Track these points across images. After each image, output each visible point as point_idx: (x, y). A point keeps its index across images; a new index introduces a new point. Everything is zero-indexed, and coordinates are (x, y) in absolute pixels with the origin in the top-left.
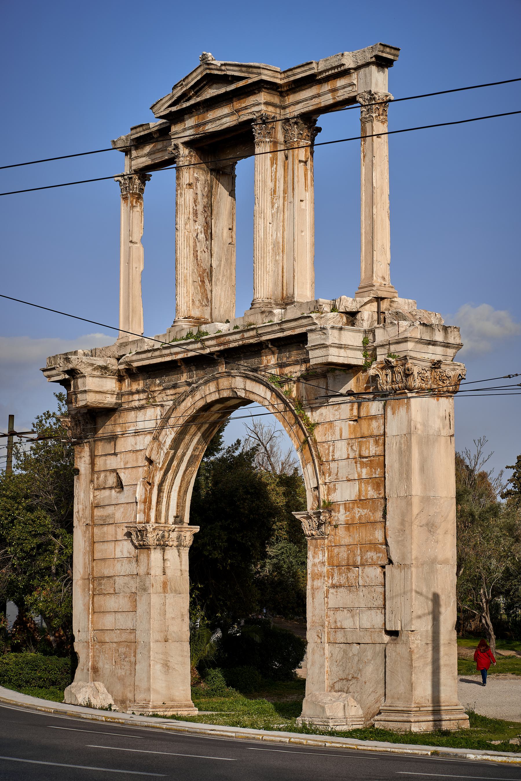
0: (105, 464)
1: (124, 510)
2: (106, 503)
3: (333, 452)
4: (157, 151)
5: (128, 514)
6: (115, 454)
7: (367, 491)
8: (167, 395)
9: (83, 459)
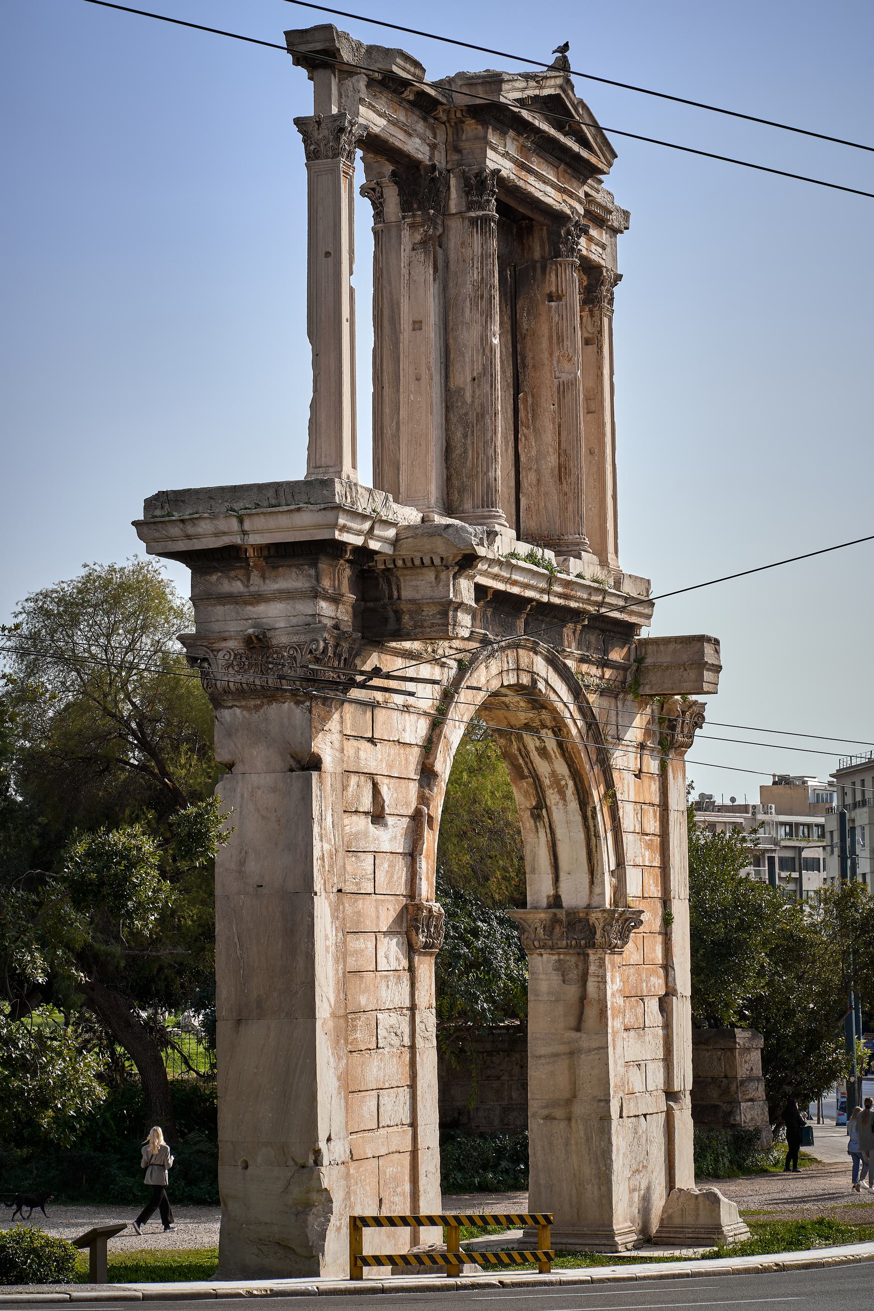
1: (389, 867)
2: (362, 845)
4: (400, 124)
5: (395, 878)
6: (372, 740)
8: (451, 647)
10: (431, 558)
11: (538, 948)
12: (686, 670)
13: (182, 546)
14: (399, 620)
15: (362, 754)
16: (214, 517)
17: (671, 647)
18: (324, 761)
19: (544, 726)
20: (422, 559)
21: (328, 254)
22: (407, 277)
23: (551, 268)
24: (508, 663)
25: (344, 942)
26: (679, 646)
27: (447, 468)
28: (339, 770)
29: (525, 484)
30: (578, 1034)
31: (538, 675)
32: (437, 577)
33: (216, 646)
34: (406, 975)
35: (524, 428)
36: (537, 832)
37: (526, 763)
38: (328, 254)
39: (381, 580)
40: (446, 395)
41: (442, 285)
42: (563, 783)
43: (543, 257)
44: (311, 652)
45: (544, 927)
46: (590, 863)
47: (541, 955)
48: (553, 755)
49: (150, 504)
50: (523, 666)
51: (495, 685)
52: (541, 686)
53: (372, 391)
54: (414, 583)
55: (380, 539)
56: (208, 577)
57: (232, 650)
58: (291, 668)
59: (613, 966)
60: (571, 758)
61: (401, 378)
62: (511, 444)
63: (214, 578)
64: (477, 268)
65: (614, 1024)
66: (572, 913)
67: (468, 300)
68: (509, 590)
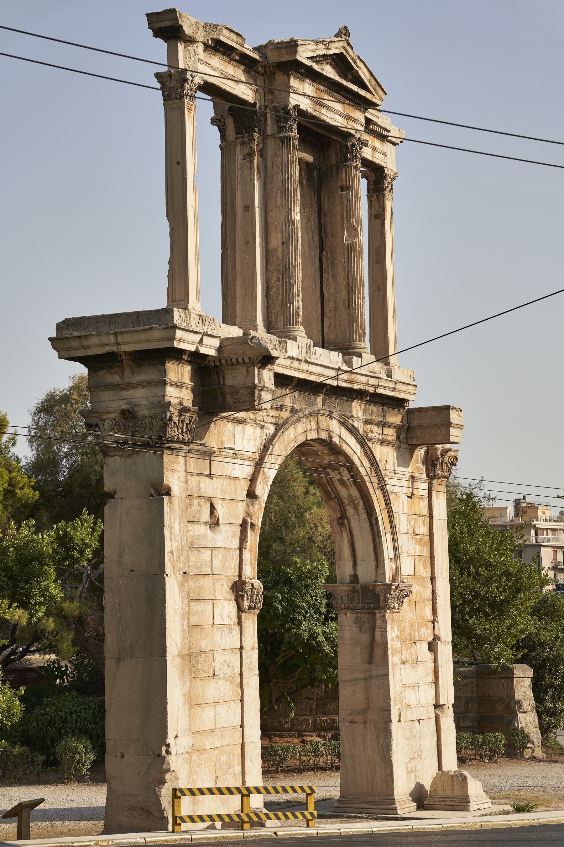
0: (199, 487)
1: (223, 557)
2: (202, 543)
3: (399, 524)
5: (227, 564)
6: (210, 476)
7: (420, 568)
8: (268, 415)
9: (176, 475)
10: (243, 359)
11: (344, 609)
12: (439, 428)
13: (80, 353)
14: (224, 398)
15: (202, 485)
16: (99, 334)
17: (430, 413)
18: (172, 489)
19: (342, 466)
20: (237, 359)
21: (178, 163)
22: (239, 177)
23: (342, 169)
24: (311, 425)
25: (189, 606)
26: (434, 413)
27: (267, 301)
28: (184, 495)
29: (327, 310)
30: (370, 666)
31: (333, 433)
32: (247, 370)
33: (104, 417)
34: (237, 628)
35: (326, 274)
36: (342, 534)
37: (332, 490)
38: (178, 163)
39: (213, 373)
40: (266, 253)
41: (262, 183)
42: (356, 502)
43: (337, 163)
44: (162, 420)
45: (348, 596)
46: (376, 553)
47: (346, 614)
48: (349, 484)
49: (60, 327)
50: (322, 426)
51: (301, 439)
52: (336, 440)
53: (221, 251)
54: (233, 375)
55: (208, 346)
56: (98, 373)
57: (114, 419)
58: (150, 430)
59: (393, 621)
60: (360, 486)
61: (237, 243)
62: (318, 284)
63: (102, 373)
64: (285, 171)
65: (393, 659)
66: (365, 587)
67: (279, 191)
68: (307, 378)
